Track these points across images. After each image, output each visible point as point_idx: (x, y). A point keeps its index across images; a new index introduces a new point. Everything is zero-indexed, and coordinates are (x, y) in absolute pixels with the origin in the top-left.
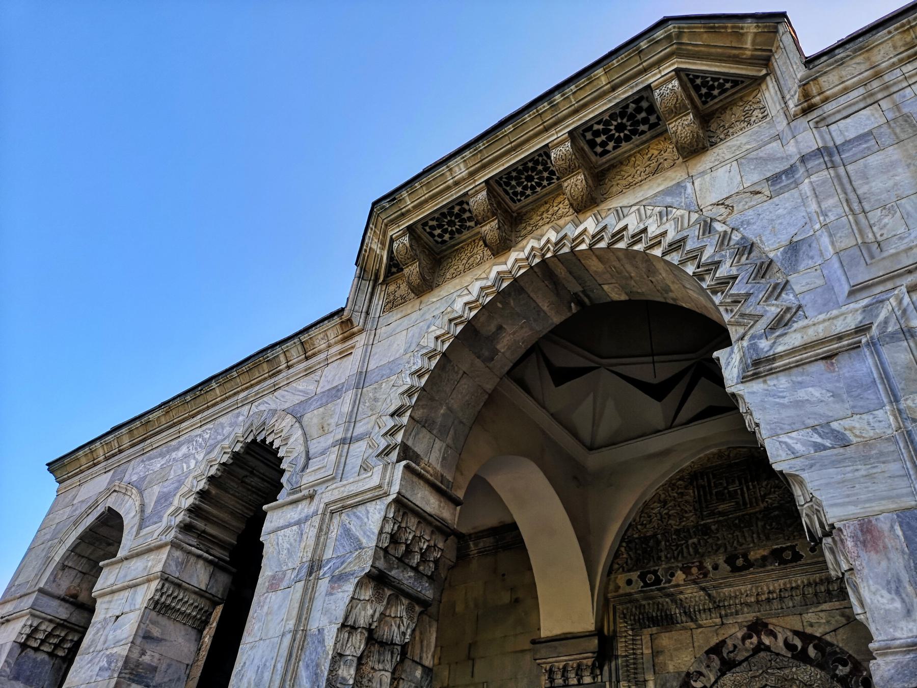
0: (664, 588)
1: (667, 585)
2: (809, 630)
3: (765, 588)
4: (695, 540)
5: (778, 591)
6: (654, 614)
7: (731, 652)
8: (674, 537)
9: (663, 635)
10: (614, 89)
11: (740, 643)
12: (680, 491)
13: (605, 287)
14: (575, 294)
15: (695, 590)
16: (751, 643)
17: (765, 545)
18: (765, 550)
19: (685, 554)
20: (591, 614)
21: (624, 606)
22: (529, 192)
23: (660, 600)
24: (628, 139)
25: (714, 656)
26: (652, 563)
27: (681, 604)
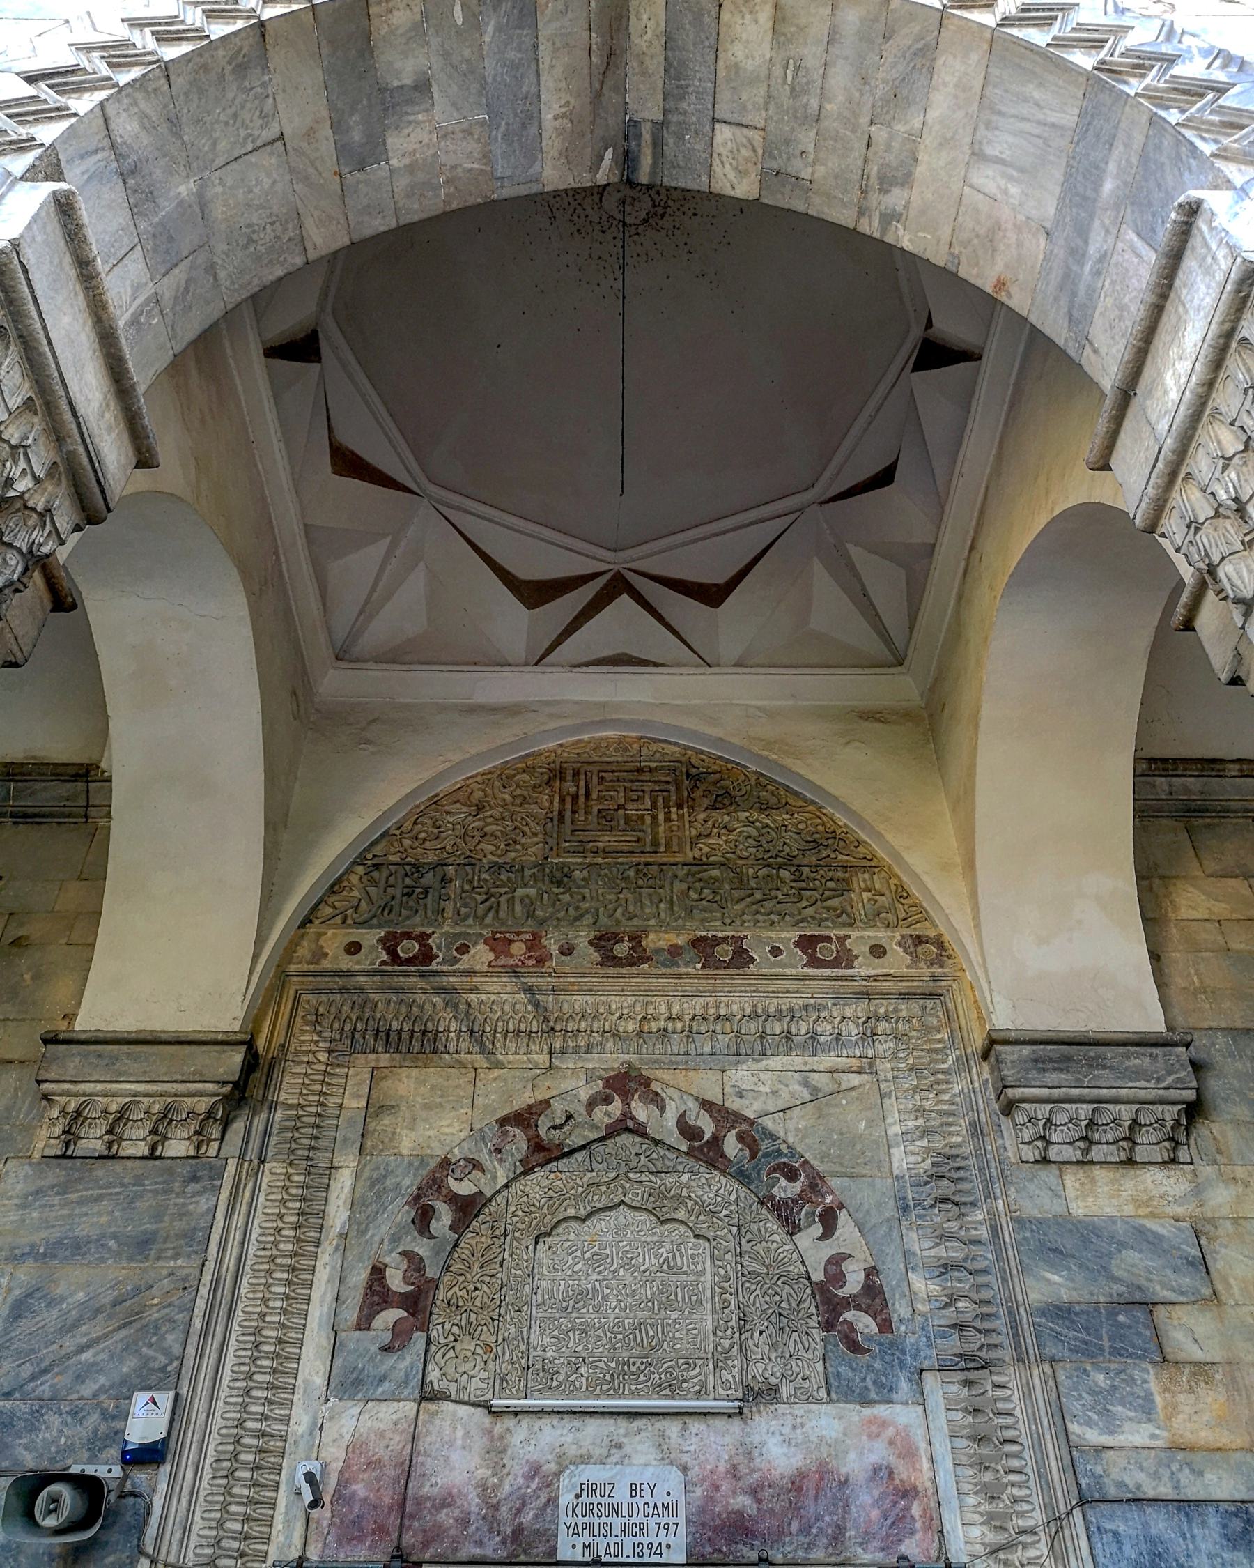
0: (436, 973)
1: (445, 968)
2: (734, 1104)
3: (663, 1009)
4: (532, 892)
5: (687, 1018)
6: (395, 1026)
7: (555, 1127)
8: (484, 876)
9: (404, 1072)
11: (583, 1110)
12: (518, 792)
15: (509, 989)
16: (606, 1114)
17: (683, 927)
18: (678, 935)
19: (502, 914)
20: (240, 998)
21: (324, 998)
23: (420, 998)
25: (517, 1131)
26: (417, 919)
27: (467, 1014)
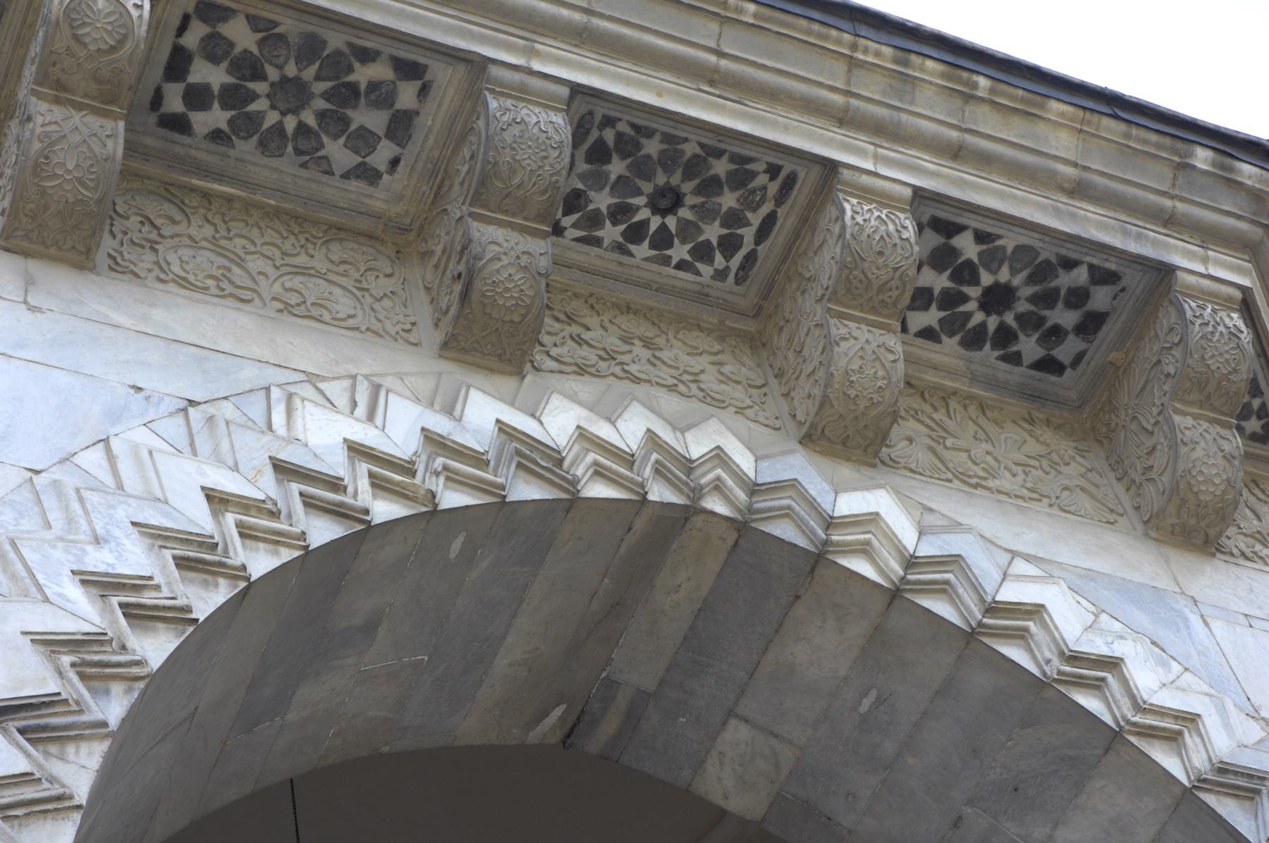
10: (1079, 190)
13: (736, 733)
14: (611, 685)
22: (611, 233)
24: (974, 340)
